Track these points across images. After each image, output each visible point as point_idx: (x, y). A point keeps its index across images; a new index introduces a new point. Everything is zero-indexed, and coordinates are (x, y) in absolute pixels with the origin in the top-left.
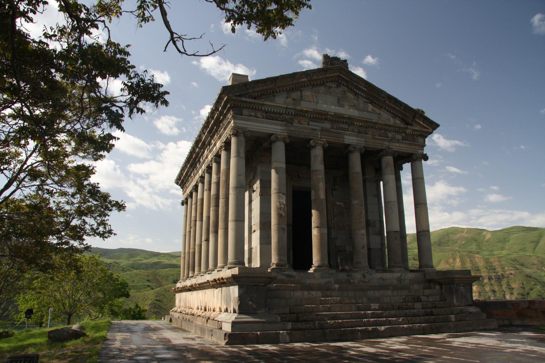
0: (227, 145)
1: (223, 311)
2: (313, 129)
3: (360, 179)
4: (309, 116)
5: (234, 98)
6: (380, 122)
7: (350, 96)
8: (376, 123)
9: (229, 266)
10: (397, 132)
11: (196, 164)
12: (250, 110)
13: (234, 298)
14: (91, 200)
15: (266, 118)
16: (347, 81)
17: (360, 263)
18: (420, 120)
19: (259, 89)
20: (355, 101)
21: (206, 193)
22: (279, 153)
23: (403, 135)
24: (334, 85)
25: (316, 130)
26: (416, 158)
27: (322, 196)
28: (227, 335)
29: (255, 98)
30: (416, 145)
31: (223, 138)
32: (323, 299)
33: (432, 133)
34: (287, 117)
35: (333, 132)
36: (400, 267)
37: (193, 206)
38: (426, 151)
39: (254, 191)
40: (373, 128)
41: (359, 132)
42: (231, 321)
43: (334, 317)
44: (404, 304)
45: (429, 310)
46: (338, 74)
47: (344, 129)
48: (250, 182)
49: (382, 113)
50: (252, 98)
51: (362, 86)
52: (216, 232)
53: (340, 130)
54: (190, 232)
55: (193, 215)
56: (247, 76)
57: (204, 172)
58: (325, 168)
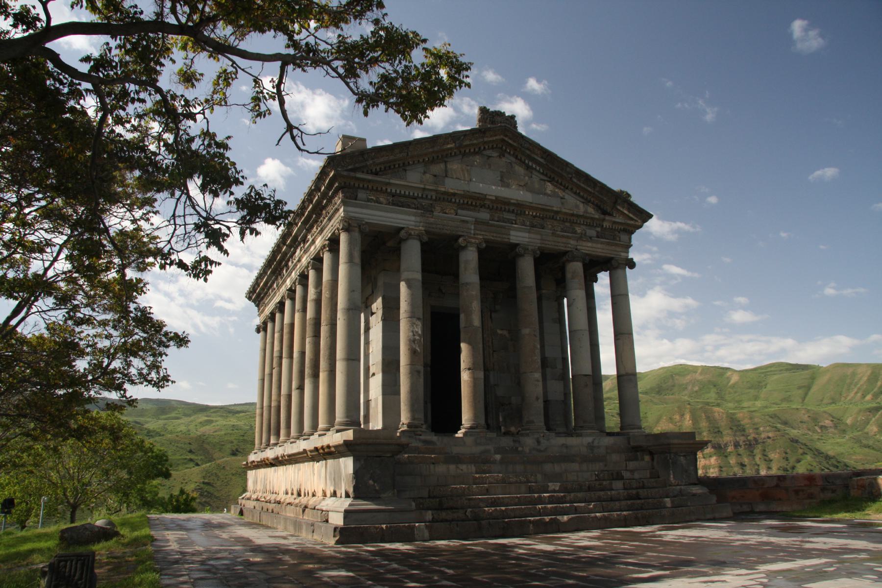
0: (333, 244)
1: (328, 494)
2: (463, 221)
3: (534, 296)
5: (345, 173)
6: (564, 210)
7: (520, 170)
8: (557, 212)
9: (336, 427)
11: (282, 269)
12: (368, 192)
13: (346, 476)
14: (137, 331)
15: (393, 204)
16: (515, 149)
17: (532, 422)
19: (382, 160)
21: (297, 316)
22: (412, 256)
23: (599, 229)
24: (495, 154)
25: (467, 222)
26: (618, 265)
27: (476, 321)
28: (338, 530)
29: (376, 174)
30: (617, 245)
31: (327, 233)
32: (477, 476)
33: (641, 227)
34: (425, 202)
35: (492, 225)
36: (591, 428)
37: (277, 335)
38: (633, 254)
39: (373, 314)
41: (533, 226)
42: (343, 510)
43: (494, 503)
44: (598, 483)
45: (634, 492)
46: (502, 137)
47: (511, 222)
48: (367, 298)
49: (567, 196)
50: (372, 173)
51: (537, 155)
52: (316, 376)
53: (504, 222)
54: (271, 375)
55: (276, 348)
56: (364, 140)
57: (294, 283)
58: (481, 279)
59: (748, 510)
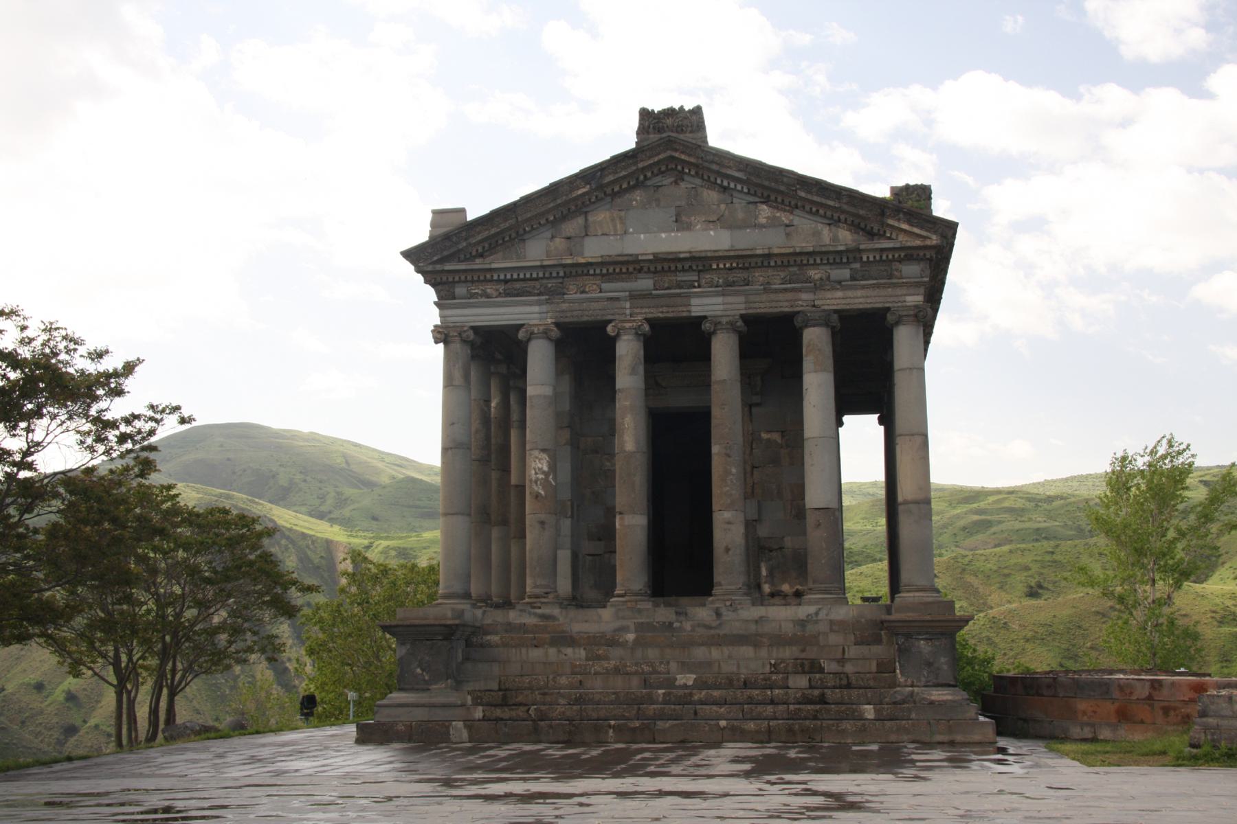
4: (598, 271)
7: (711, 196)
8: (769, 256)
10: (835, 263)
16: (696, 166)
17: (720, 585)
18: (899, 220)
19: (479, 238)
20: (723, 206)
23: (857, 266)
25: (617, 299)
29: (481, 256)
30: (894, 285)
35: (658, 296)
40: (763, 266)
45: (816, 692)
46: (669, 153)
49: (796, 221)
51: (730, 167)
56: (463, 211)
59: (1090, 736)
